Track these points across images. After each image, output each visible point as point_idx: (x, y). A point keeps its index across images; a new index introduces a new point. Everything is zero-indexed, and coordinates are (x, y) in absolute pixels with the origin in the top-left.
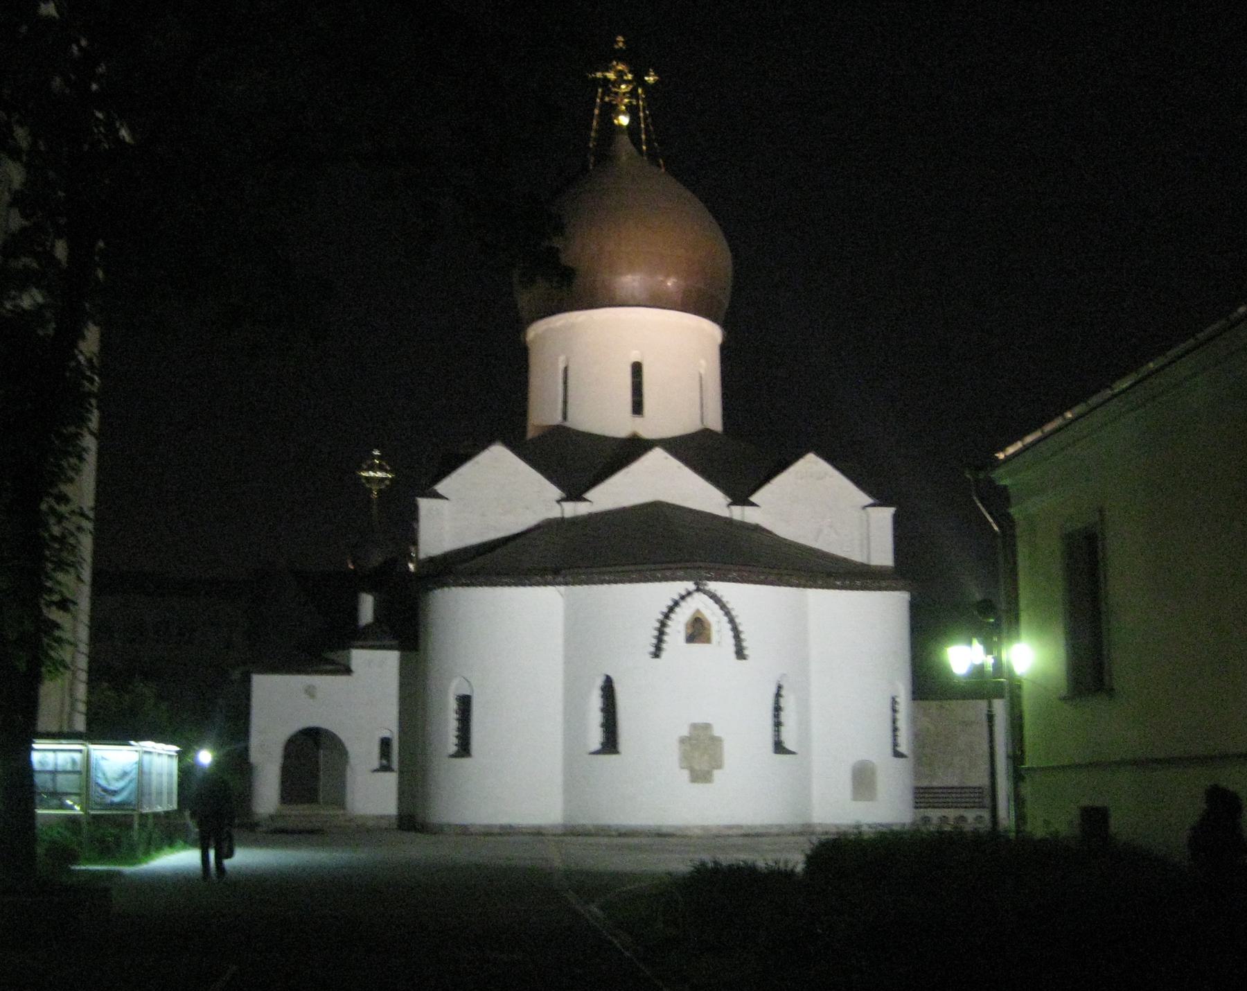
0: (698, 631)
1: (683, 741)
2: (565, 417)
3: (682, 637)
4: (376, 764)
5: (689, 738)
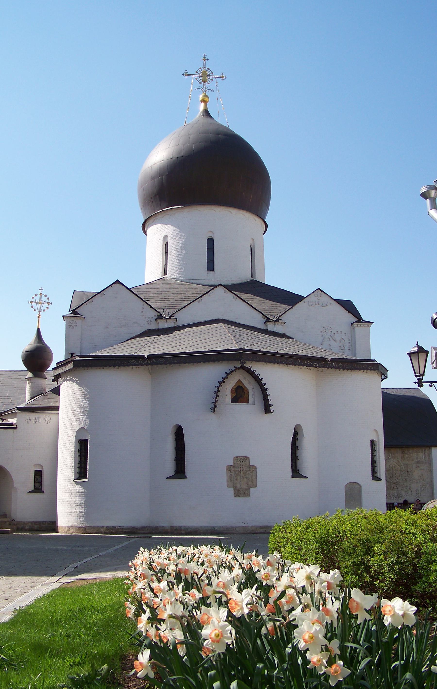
0: (239, 396)
1: (229, 468)
3: (228, 399)
4: (32, 488)
5: (234, 467)
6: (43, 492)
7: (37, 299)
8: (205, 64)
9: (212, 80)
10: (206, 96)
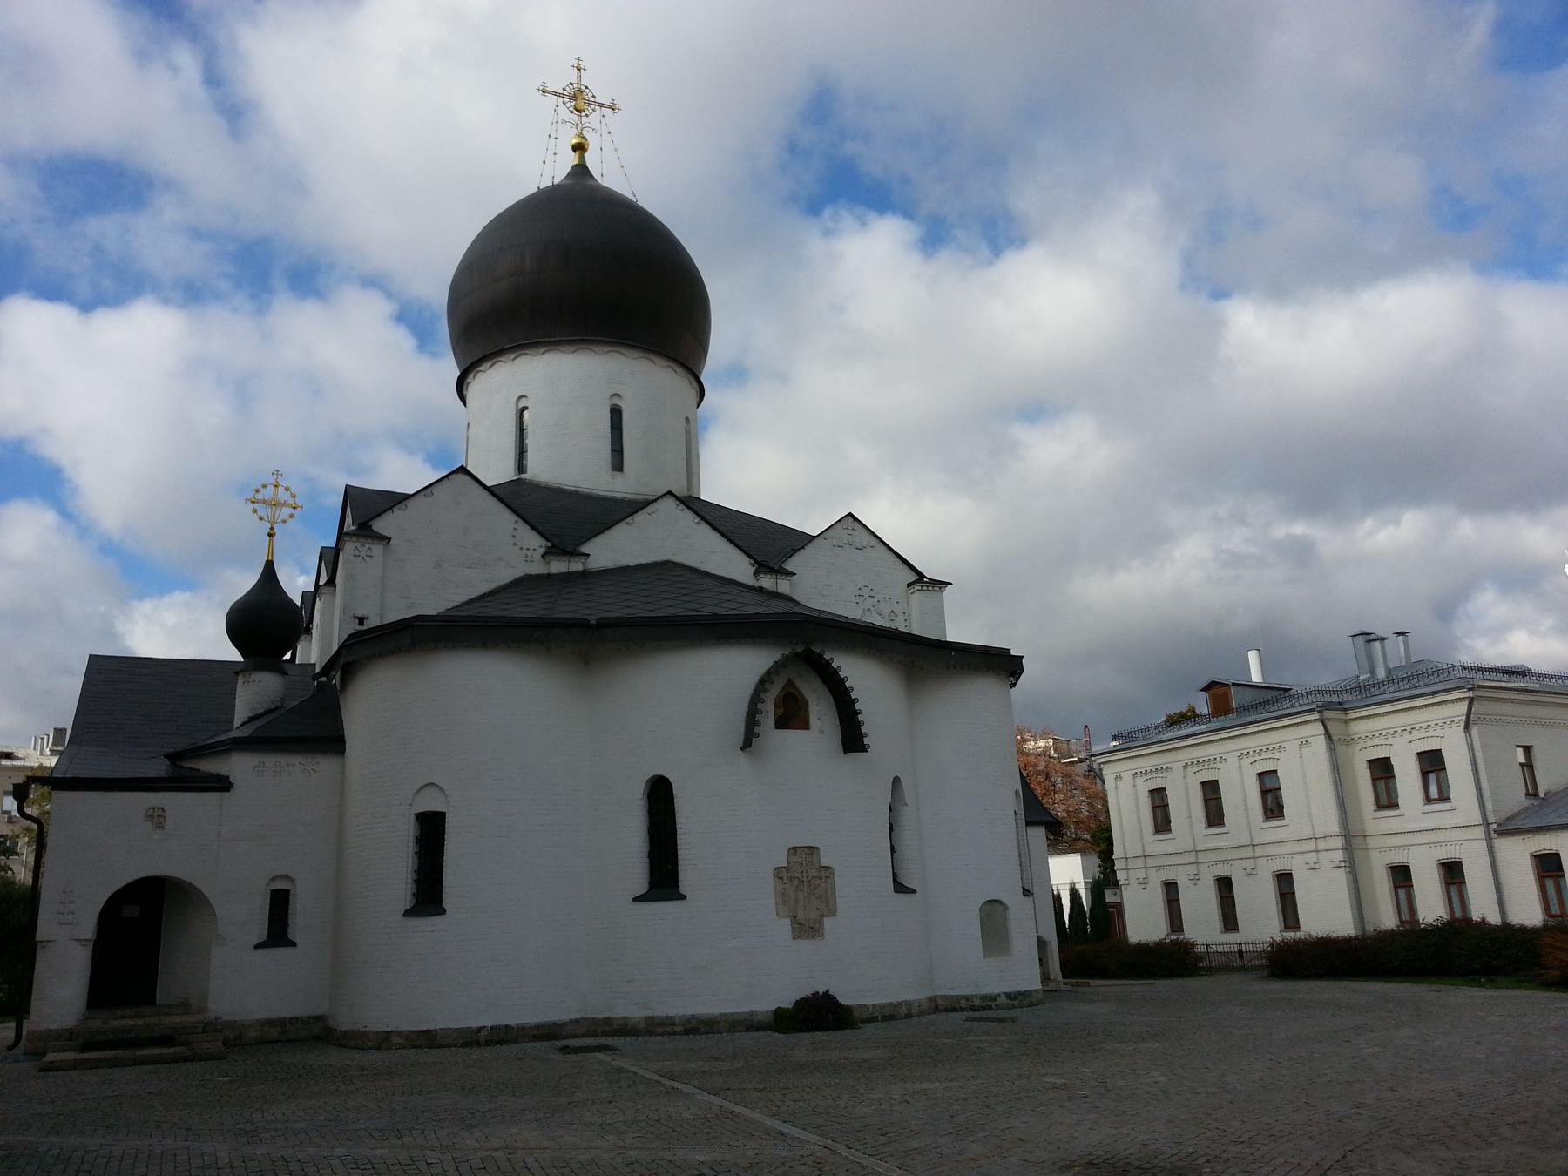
0: (792, 715)
2: (521, 467)
3: (771, 721)
6: (294, 944)
7: (268, 493)
8: (579, 77)
10: (581, 135)
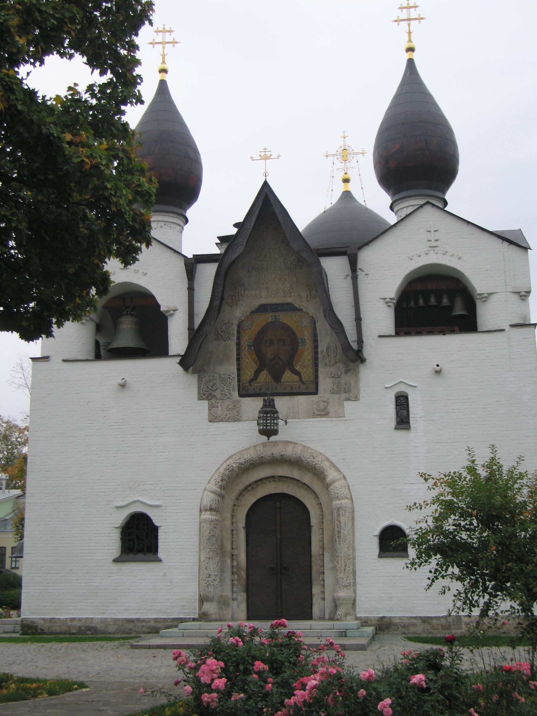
8: (344, 142)
9: (353, 158)
